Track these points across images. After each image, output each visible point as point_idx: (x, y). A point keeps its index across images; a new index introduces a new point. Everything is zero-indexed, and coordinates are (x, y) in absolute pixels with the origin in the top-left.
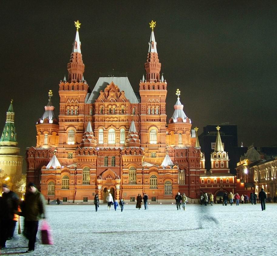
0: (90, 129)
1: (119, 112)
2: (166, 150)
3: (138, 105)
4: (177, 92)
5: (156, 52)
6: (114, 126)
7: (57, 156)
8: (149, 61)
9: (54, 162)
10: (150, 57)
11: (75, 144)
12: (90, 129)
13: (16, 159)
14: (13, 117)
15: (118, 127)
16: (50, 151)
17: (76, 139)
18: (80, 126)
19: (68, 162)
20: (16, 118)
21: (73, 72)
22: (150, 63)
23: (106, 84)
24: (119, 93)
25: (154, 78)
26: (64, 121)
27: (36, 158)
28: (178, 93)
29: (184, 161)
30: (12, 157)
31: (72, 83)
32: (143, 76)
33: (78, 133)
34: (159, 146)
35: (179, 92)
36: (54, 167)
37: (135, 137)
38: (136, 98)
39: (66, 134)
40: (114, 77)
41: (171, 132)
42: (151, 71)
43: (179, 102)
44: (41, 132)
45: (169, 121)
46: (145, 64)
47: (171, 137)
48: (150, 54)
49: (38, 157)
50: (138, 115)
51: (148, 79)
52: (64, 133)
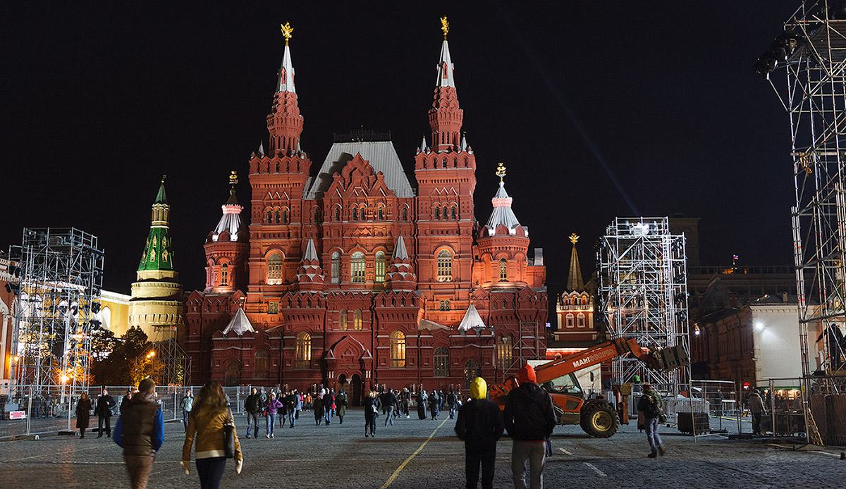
0: (311, 252)
1: (372, 216)
2: (471, 294)
3: (413, 200)
4: (499, 168)
5: (452, 85)
6: (361, 245)
7: (246, 309)
8: (438, 106)
9: (238, 322)
10: (438, 97)
11: (282, 284)
12: (311, 252)
13: (175, 308)
14: (166, 216)
15: (370, 248)
16: (231, 300)
17: (285, 274)
18: (293, 247)
19: (269, 321)
20: (172, 218)
21: (279, 133)
22: (439, 110)
23: (346, 157)
24: (372, 176)
25: (448, 143)
26: (259, 236)
27: (203, 313)
28: (501, 171)
29: (509, 317)
30: (165, 304)
31: (276, 157)
32: (424, 139)
33: (289, 260)
34: (457, 286)
35: (504, 168)
36: (240, 331)
37: (405, 270)
38: (409, 186)
39: (264, 263)
40: (364, 141)
41: (485, 256)
42: (442, 128)
43: (502, 191)
44: (214, 259)
45: (479, 235)
46: (429, 112)
47: (484, 267)
48: (439, 91)
49: (208, 312)
50: (413, 222)
51: (433, 145)
52: (261, 261)
